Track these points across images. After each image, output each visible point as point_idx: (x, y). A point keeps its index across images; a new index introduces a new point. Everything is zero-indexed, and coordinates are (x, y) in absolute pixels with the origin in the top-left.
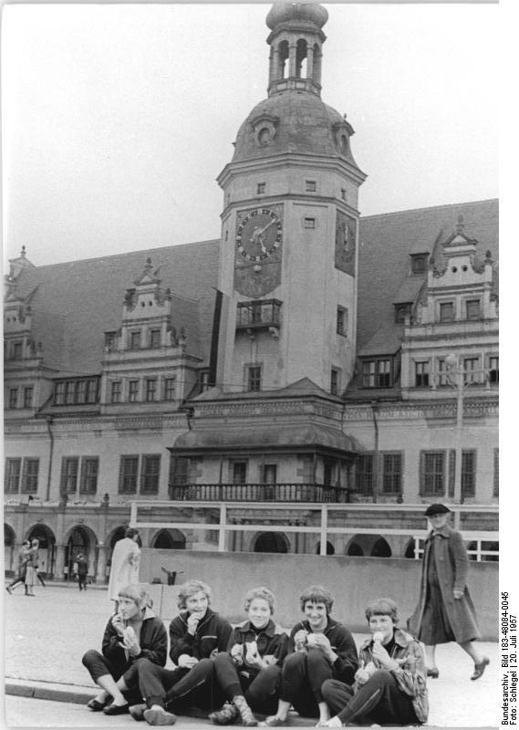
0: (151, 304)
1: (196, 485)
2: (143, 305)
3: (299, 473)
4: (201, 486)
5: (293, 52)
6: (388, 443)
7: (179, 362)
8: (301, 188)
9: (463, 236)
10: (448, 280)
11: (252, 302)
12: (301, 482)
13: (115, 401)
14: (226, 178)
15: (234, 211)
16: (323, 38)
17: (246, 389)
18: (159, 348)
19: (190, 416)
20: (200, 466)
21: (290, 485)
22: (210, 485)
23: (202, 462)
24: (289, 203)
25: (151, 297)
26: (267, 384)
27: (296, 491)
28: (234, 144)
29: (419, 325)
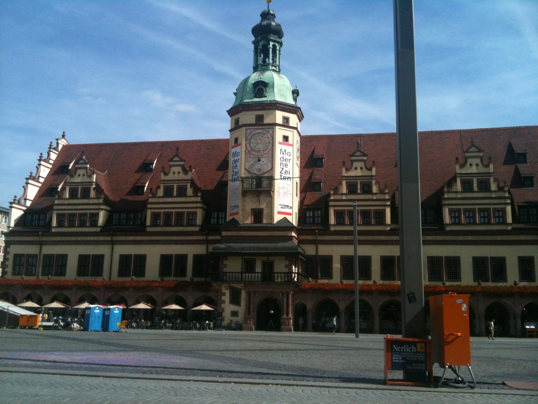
0: (179, 173)
1: (224, 273)
2: (174, 173)
3: (286, 266)
4: (226, 273)
5: (271, 50)
6: (324, 250)
7: (199, 205)
9: (361, 152)
10: (352, 173)
14: (231, 112)
15: (244, 129)
16: (281, 44)
17: (253, 222)
18: (185, 196)
19: (220, 234)
20: (225, 262)
21: (281, 273)
22: (235, 273)
23: (226, 259)
25: (179, 169)
27: (284, 276)
28: (235, 94)
29: (338, 194)
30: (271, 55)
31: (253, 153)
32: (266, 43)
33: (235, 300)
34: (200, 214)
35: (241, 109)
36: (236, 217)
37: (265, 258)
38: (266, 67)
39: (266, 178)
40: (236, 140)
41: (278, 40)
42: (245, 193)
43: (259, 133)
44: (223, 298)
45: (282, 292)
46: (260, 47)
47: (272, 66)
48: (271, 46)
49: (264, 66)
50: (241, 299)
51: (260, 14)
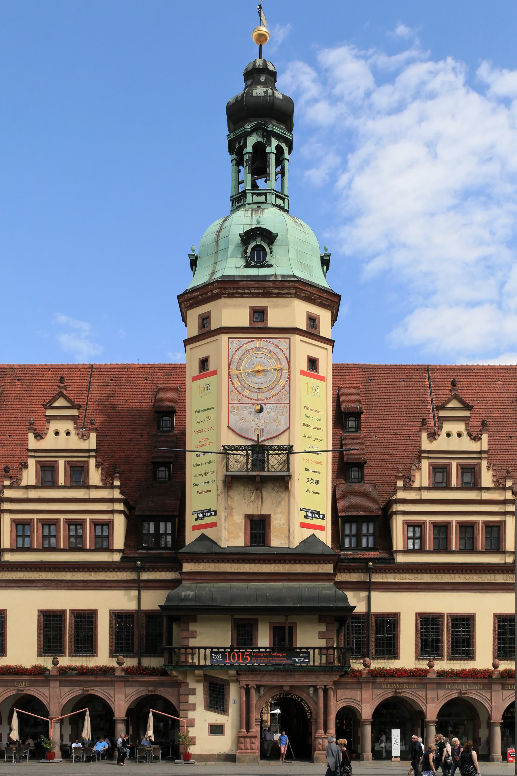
4: (193, 648)
8: (303, 325)
11: (251, 446)
12: (324, 645)
13: (27, 545)
15: (224, 337)
17: (248, 544)
19: (179, 569)
20: (192, 627)
23: (195, 620)
24: (297, 338)
26: (276, 541)
27: (320, 654)
30: (273, 169)
31: (246, 393)
32: (260, 139)
33: (217, 701)
34: (120, 523)
35: (215, 291)
36: (209, 533)
37: (279, 620)
38: (262, 198)
39: (279, 448)
40: (204, 363)
41: (288, 135)
42: (231, 482)
43: (258, 349)
44: (191, 699)
45: (315, 687)
46: (249, 149)
47: (277, 196)
48: (272, 149)
49: (259, 194)
50: (228, 701)
51: (243, 71)
